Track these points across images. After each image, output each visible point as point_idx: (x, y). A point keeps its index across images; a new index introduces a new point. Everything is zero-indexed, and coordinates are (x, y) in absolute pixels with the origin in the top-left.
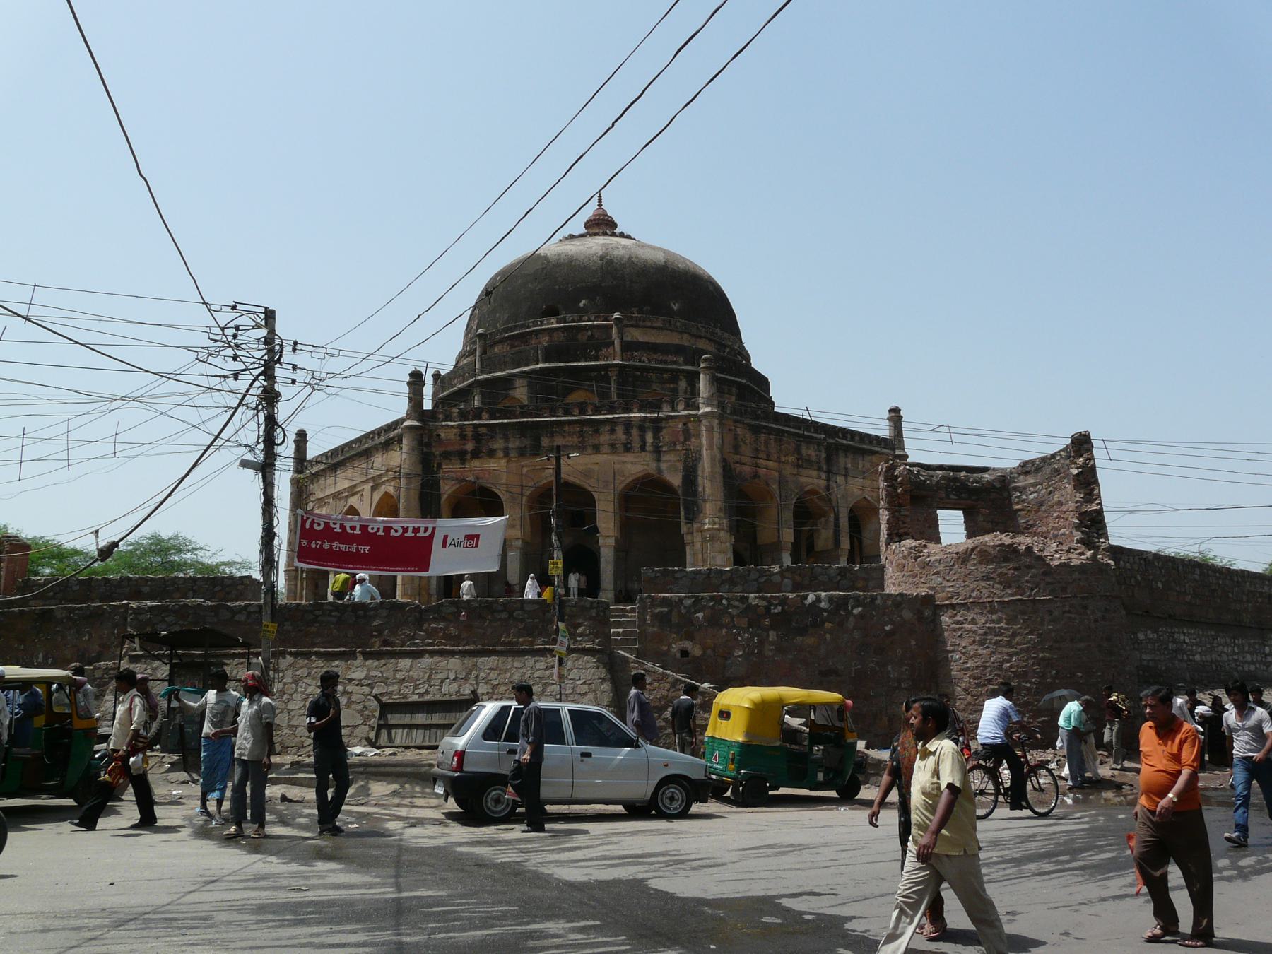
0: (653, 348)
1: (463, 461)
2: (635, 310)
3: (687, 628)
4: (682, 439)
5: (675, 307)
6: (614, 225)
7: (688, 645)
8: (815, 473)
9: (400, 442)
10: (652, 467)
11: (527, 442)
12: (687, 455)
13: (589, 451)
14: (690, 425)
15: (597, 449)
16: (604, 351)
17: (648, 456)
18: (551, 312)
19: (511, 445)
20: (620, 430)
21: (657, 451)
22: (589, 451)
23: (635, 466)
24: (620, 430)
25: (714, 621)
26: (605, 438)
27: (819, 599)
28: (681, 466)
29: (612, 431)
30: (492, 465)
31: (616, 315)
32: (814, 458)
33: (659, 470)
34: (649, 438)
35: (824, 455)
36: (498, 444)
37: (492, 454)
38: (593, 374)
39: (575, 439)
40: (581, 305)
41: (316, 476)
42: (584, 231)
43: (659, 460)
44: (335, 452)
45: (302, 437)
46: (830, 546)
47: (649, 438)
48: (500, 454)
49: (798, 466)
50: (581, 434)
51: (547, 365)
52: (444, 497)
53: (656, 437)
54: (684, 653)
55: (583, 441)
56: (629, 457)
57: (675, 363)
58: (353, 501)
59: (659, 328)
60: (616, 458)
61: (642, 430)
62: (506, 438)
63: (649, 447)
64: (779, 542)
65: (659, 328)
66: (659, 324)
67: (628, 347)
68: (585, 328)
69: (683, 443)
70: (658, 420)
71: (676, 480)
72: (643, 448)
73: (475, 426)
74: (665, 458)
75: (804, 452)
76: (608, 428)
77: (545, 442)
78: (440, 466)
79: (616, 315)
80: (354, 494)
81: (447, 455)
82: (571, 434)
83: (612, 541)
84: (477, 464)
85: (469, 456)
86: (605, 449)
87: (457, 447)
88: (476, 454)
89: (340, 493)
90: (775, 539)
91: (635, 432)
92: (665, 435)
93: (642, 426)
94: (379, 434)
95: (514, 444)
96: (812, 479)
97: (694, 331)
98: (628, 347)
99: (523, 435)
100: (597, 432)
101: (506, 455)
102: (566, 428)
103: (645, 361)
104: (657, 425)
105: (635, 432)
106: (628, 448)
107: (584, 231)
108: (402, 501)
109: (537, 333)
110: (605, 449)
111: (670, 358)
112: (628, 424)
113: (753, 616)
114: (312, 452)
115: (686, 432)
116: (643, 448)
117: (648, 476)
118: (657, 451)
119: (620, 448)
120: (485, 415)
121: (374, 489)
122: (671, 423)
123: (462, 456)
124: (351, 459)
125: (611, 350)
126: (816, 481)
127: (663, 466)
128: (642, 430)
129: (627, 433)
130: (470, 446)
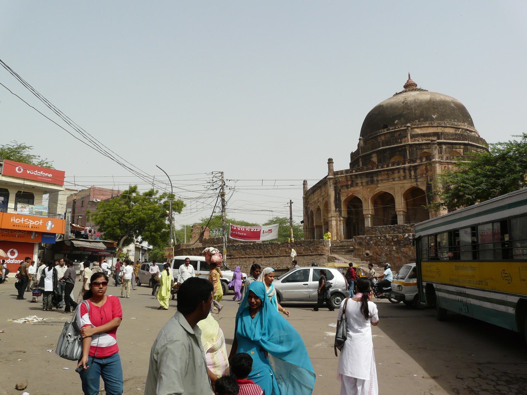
0: (424, 135)
1: (348, 188)
2: (417, 121)
3: (368, 246)
4: (425, 172)
5: (434, 117)
6: (416, 85)
7: (368, 252)
10: (414, 184)
11: (369, 179)
13: (391, 180)
14: (428, 167)
15: (394, 180)
17: (413, 180)
18: (386, 127)
19: (363, 181)
20: (401, 171)
22: (391, 180)
23: (408, 184)
24: (401, 171)
25: (376, 244)
26: (396, 175)
27: (409, 236)
28: (425, 183)
29: (399, 172)
30: (357, 189)
33: (417, 184)
34: (413, 173)
36: (359, 181)
37: (357, 185)
38: (400, 149)
42: (403, 89)
43: (417, 181)
45: (305, 183)
47: (413, 173)
48: (360, 184)
50: (387, 174)
53: (415, 173)
54: (367, 254)
56: (405, 181)
59: (427, 127)
60: (401, 182)
61: (410, 170)
65: (427, 127)
66: (427, 125)
67: (413, 136)
68: (397, 131)
70: (416, 166)
71: (424, 188)
73: (351, 176)
74: (419, 180)
77: (375, 178)
78: (340, 190)
80: (318, 202)
81: (342, 186)
82: (384, 175)
84: (352, 189)
86: (397, 179)
87: (345, 184)
88: (352, 186)
91: (407, 172)
92: (419, 171)
93: (410, 168)
95: (364, 180)
97: (443, 125)
98: (413, 136)
99: (367, 177)
100: (393, 173)
101: (362, 185)
102: (382, 173)
104: (415, 168)
105: (407, 172)
106: (405, 178)
107: (403, 89)
109: (380, 135)
110: (397, 179)
112: (404, 169)
113: (388, 242)
115: (426, 169)
116: (410, 177)
119: (402, 178)
120: (354, 171)
121: (323, 199)
122: (421, 167)
123: (347, 186)
125: (406, 139)
127: (419, 183)
128: (410, 170)
129: (404, 172)
130: (349, 183)
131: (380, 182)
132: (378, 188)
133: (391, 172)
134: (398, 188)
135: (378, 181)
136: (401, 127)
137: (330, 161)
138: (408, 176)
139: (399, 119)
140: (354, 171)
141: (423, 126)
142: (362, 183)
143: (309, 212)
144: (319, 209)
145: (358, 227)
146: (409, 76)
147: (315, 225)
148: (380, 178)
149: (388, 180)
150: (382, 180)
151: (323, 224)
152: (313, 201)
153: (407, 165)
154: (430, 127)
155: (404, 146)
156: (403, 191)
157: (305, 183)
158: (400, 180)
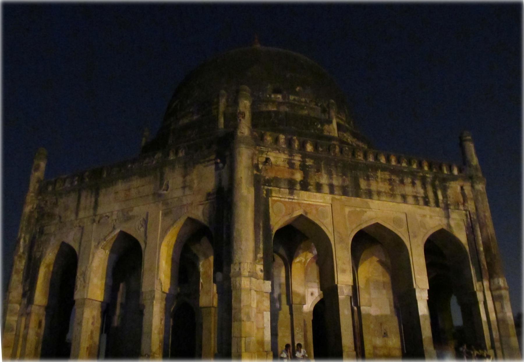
4: (461, 200)
19: (335, 182)
22: (399, 199)
23: (432, 220)
33: (449, 225)
37: (319, 188)
48: (326, 189)
53: (445, 196)
56: (426, 210)
62: (330, 174)
63: (442, 205)
69: (464, 204)
71: (462, 237)
77: (363, 184)
85: (298, 187)
87: (287, 176)
88: (305, 186)
101: (332, 192)
127: (452, 223)
130: (298, 176)
149: (392, 195)
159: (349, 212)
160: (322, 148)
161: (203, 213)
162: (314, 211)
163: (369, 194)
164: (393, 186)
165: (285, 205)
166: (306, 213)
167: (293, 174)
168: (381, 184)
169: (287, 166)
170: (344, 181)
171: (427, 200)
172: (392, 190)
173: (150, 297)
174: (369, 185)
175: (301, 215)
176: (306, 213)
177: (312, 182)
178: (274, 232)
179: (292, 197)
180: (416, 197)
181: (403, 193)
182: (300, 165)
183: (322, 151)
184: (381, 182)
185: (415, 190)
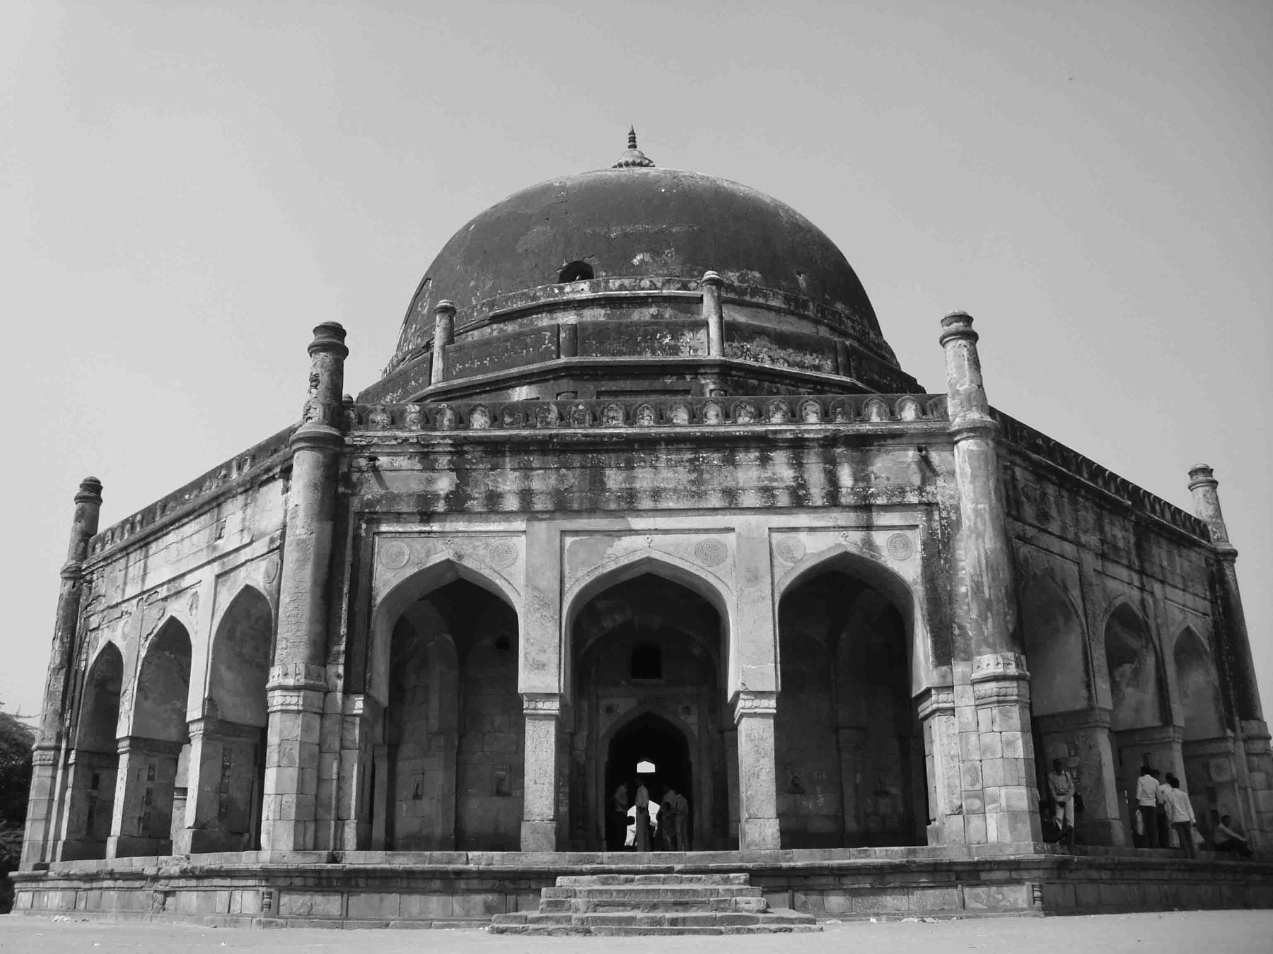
4: (917, 480)
8: (1123, 573)
9: (287, 473)
10: (851, 542)
11: (572, 478)
12: (929, 515)
16: (688, 337)
19: (537, 485)
20: (780, 458)
21: (865, 506)
22: (715, 501)
24: (780, 458)
28: (916, 538)
29: (764, 461)
31: (710, 274)
32: (1121, 544)
33: (869, 543)
35: (1132, 539)
36: (509, 483)
39: (682, 476)
40: (636, 261)
41: (109, 559)
44: (148, 513)
45: (92, 492)
46: (1150, 718)
48: (512, 503)
49: (1103, 556)
50: (694, 466)
51: (576, 359)
52: (379, 600)
55: (698, 482)
56: (802, 519)
57: (817, 368)
58: (177, 609)
59: (778, 311)
62: (527, 469)
64: (1091, 708)
67: (730, 332)
69: (921, 490)
71: (906, 565)
72: (833, 499)
75: (1107, 528)
76: (754, 455)
77: (614, 479)
79: (710, 274)
83: (770, 705)
85: (441, 507)
86: (750, 499)
87: (415, 486)
88: (457, 504)
89: (154, 590)
90: (1081, 704)
94: (240, 468)
96: (1121, 585)
103: (765, 357)
106: (799, 501)
108: (285, 599)
110: (750, 499)
111: (808, 359)
112: (797, 445)
114: (109, 518)
117: (845, 557)
118: (865, 506)
119: (783, 499)
120: (479, 421)
124: (177, 522)
125: (702, 334)
126: (1126, 589)
127: (880, 538)
129: (798, 464)
130: (444, 484)
131: (646, 504)
132: (627, 542)
133: (716, 458)
134: (742, 548)
135: (630, 496)
136: (666, 283)
137: (332, 341)
138: (817, 494)
139: (656, 253)
140: (479, 421)
141: (761, 301)
142: (526, 496)
143: (91, 656)
144: (173, 640)
145: (392, 772)
146: (633, 139)
147: (124, 728)
148: (644, 479)
150: (656, 494)
151: (196, 730)
152: (131, 591)
153: (813, 424)
154: (792, 314)
155: (695, 368)
156: (787, 575)
157: (92, 492)
158: (771, 509)
159: (573, 543)
160: (511, 415)
161: (267, 573)
162: (481, 552)
163: (629, 502)
164: (701, 472)
165: (408, 545)
166: (460, 557)
167: (430, 481)
168: (665, 473)
169: (419, 466)
170: (562, 479)
171: (802, 492)
172: (698, 482)
173: (967, 738)
174: (631, 479)
175: (448, 560)
176: (460, 557)
177: (477, 495)
178: (379, 600)
179: (427, 529)
180: (767, 491)
181: (730, 484)
182: (450, 462)
183: (512, 423)
184: (668, 467)
185: (769, 474)
